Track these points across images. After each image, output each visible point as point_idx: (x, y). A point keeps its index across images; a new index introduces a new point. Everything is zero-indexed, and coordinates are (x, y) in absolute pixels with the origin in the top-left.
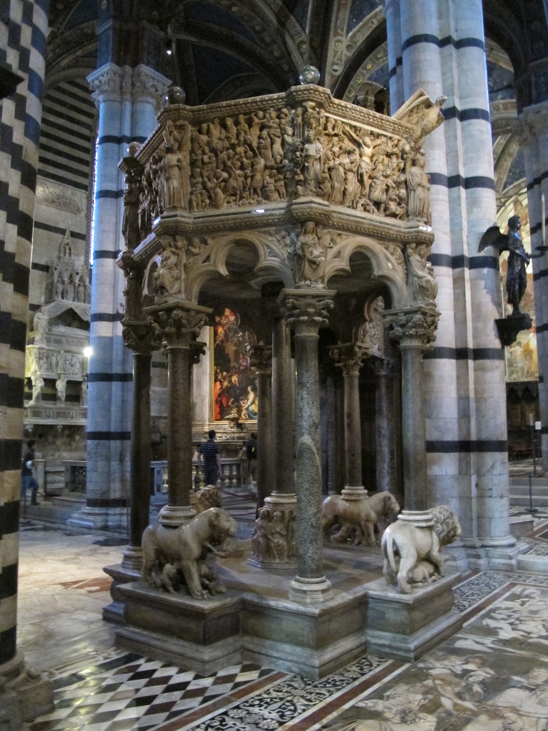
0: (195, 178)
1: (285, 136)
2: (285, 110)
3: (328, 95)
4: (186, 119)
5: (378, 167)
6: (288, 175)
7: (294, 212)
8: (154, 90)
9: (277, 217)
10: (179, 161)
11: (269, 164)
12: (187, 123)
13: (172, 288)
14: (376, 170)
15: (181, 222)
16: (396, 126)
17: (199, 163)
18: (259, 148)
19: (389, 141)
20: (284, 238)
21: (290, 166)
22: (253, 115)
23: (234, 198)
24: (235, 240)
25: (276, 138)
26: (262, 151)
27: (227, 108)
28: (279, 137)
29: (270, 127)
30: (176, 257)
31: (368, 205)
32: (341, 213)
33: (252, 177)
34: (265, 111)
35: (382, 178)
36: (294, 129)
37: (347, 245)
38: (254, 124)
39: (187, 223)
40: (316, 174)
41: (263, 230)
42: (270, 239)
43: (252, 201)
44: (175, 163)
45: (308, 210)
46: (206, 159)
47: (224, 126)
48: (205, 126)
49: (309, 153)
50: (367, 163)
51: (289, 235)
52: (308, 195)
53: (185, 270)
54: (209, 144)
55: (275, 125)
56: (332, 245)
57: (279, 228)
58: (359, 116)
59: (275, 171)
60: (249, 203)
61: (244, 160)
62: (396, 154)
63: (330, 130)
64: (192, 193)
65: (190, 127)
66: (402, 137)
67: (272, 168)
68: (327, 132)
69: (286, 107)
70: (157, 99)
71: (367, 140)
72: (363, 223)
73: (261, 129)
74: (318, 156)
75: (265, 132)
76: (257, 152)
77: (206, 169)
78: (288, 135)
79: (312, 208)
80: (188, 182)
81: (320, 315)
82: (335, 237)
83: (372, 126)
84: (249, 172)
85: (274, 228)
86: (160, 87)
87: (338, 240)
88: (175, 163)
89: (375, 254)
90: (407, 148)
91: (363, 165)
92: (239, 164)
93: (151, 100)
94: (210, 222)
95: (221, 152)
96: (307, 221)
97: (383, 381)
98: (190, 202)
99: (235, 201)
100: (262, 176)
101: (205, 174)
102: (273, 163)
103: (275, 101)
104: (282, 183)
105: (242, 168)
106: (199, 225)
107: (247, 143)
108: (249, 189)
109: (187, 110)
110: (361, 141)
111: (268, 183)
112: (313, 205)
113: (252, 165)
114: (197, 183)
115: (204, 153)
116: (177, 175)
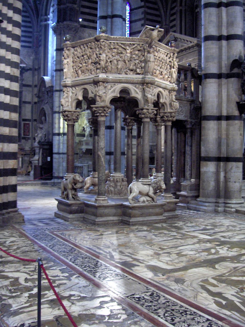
4: (70, 47)
10: (68, 62)
13: (65, 105)
31: (127, 71)
42: (92, 87)
47: (81, 48)
48: (76, 48)
50: (128, 56)
59: (94, 64)
63: (112, 47)
71: (128, 48)
81: (104, 113)
82: (112, 86)
90: (145, 48)
91: (126, 57)
97: (189, 130)
105: (86, 63)
107: (86, 54)
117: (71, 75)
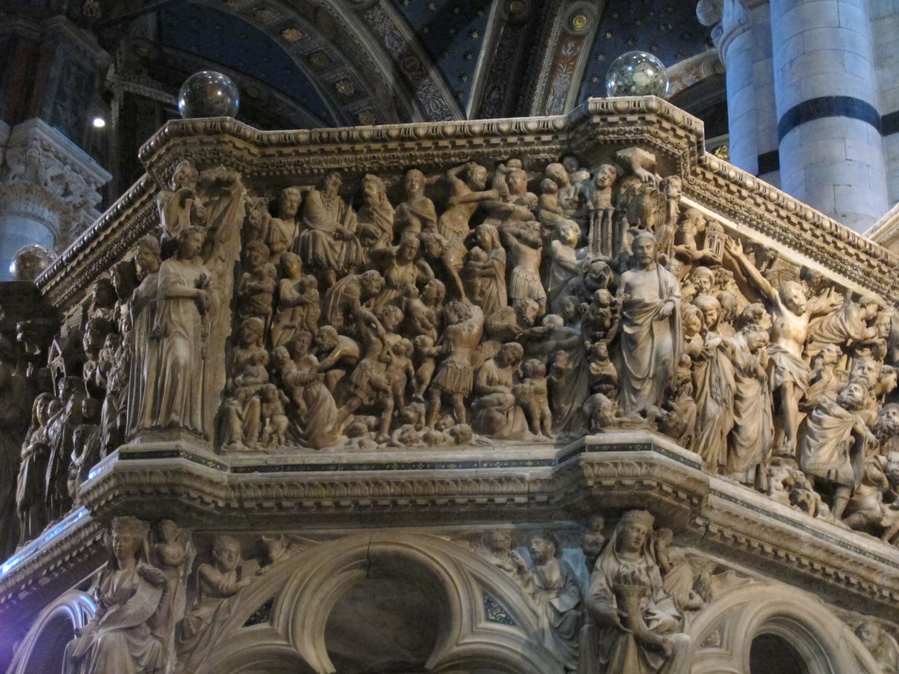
0: (245, 346)
1: (556, 243)
2: (557, 169)
3: (698, 135)
5: (825, 377)
6: (562, 360)
7: (588, 471)
8: (60, 190)
9: (524, 488)
10: (200, 284)
11: (497, 323)
12: (238, 176)
14: (818, 385)
15: (190, 474)
16: (874, 262)
17: (266, 302)
18: (466, 273)
19: (853, 307)
20: (540, 560)
21: (569, 335)
22: (453, 173)
23: (372, 419)
24: (368, 555)
25: (524, 248)
26: (479, 282)
27: (374, 146)
28: (534, 245)
29: (507, 215)
30: (158, 593)
32: (729, 498)
33: (440, 360)
34: (493, 166)
35: (839, 410)
36: (585, 227)
37: (743, 606)
38: (454, 200)
39: (211, 482)
40: (659, 359)
41: (469, 528)
42: (495, 560)
43: (435, 433)
44: (190, 288)
45: (640, 471)
46: (289, 289)
49: (636, 297)
50: (793, 359)
51: (558, 554)
52: (632, 425)
53: (178, 645)
54: (302, 247)
55: (524, 210)
56: (697, 600)
57: (525, 525)
58: (773, 217)
60: (426, 438)
61: (417, 303)
62: (872, 346)
64: (228, 393)
65: (245, 192)
66: (888, 297)
67: (506, 336)
68: (681, 248)
69: (561, 161)
70: (66, 213)
71: (797, 290)
72: (796, 538)
73: (476, 220)
74: (667, 308)
75: (489, 228)
76: (460, 283)
77: (286, 321)
78: (565, 242)
79: (652, 465)
80: (222, 355)
82: (706, 575)
83: (807, 252)
84: (430, 341)
85: (509, 526)
86: (77, 183)
87: (715, 586)
88: (190, 288)
89: (824, 651)
91: (783, 362)
92: (398, 314)
93: (47, 214)
94: (291, 485)
95: (340, 276)
96: (630, 508)
98: (222, 420)
99: (378, 428)
100: (473, 359)
101: (281, 336)
102: (512, 320)
103: (529, 139)
104: (541, 384)
105: (407, 328)
106: (250, 493)
108: (428, 395)
109: (244, 138)
110: (775, 292)
111: (490, 382)
112: (654, 455)
113: (443, 323)
114: (252, 361)
115: (284, 272)
116: (190, 326)
117: (212, 413)
